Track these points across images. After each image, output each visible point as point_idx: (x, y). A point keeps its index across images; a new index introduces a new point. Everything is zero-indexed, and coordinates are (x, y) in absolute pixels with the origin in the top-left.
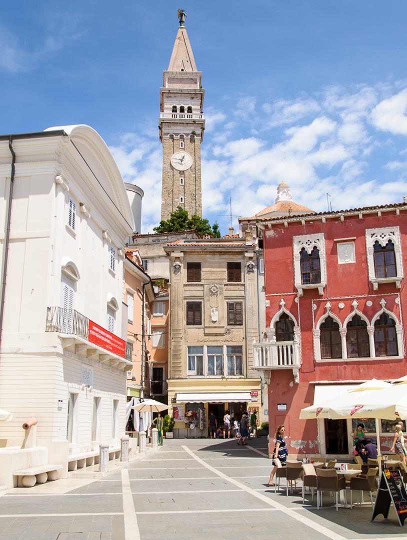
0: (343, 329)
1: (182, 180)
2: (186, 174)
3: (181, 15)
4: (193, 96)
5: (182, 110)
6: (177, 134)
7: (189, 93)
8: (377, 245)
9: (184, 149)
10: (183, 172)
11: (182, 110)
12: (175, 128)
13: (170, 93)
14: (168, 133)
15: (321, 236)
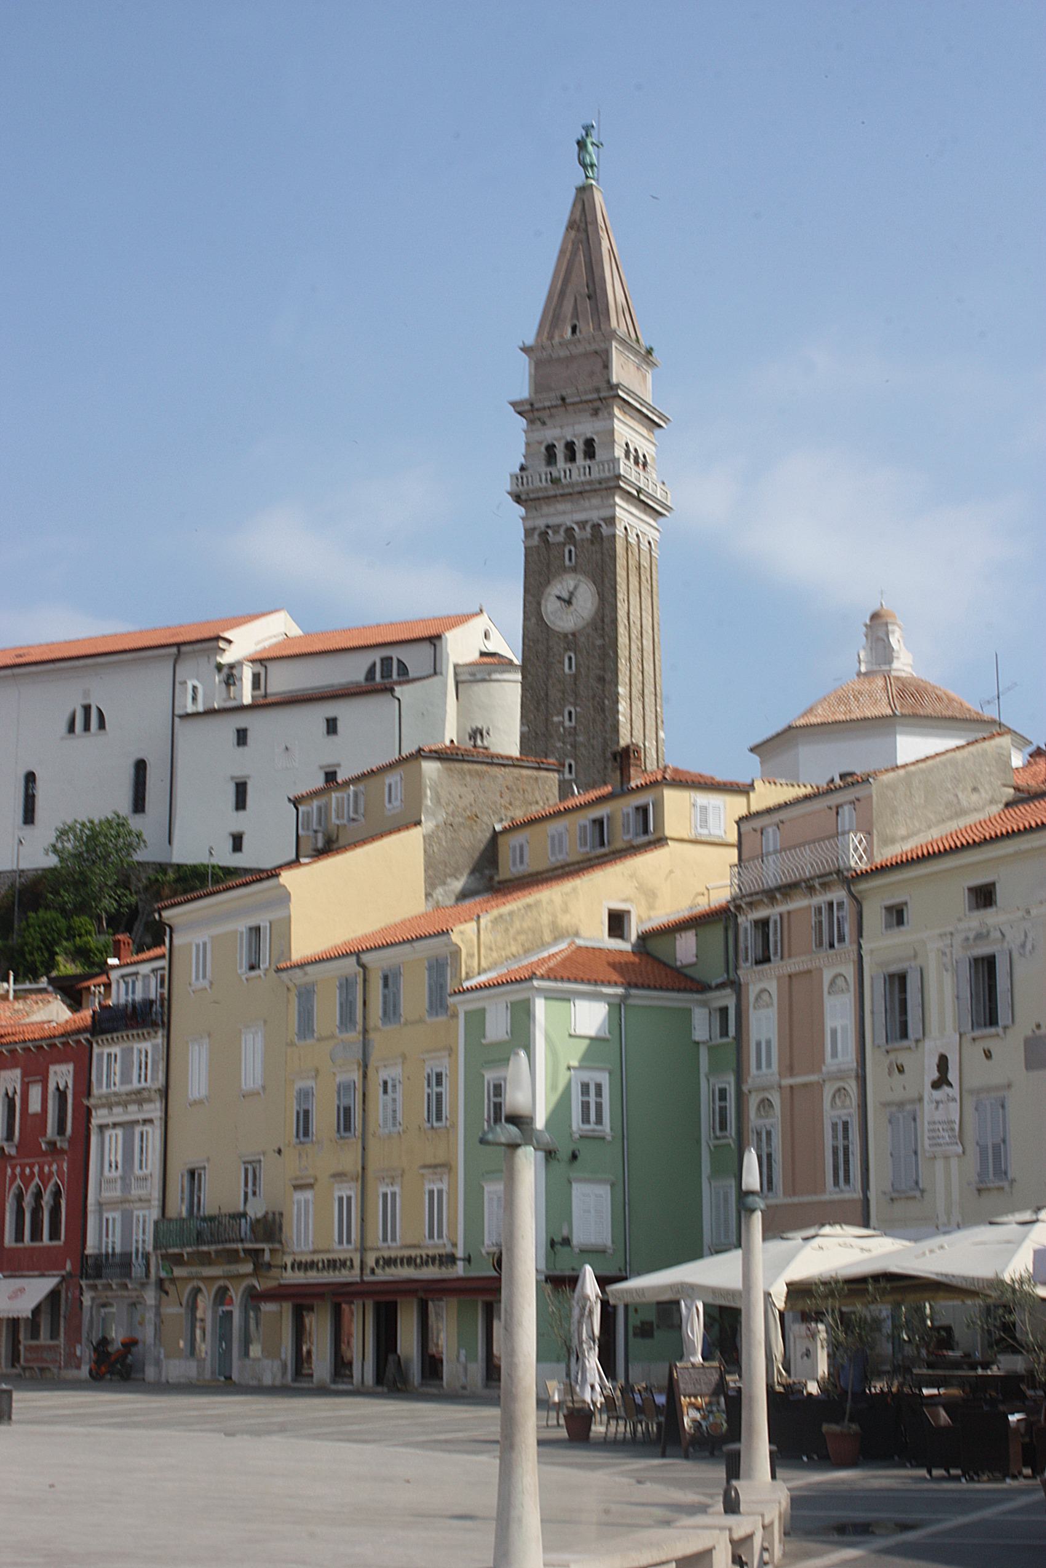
0: (28, 1200)
1: (570, 659)
2: (582, 639)
3: (581, 144)
4: (598, 404)
5: (570, 446)
6: (556, 528)
7: (586, 402)
8: (58, 1088)
9: (574, 570)
10: (574, 634)
11: (570, 446)
12: (552, 510)
13: (537, 410)
14: (534, 529)
15: (17, 1072)
